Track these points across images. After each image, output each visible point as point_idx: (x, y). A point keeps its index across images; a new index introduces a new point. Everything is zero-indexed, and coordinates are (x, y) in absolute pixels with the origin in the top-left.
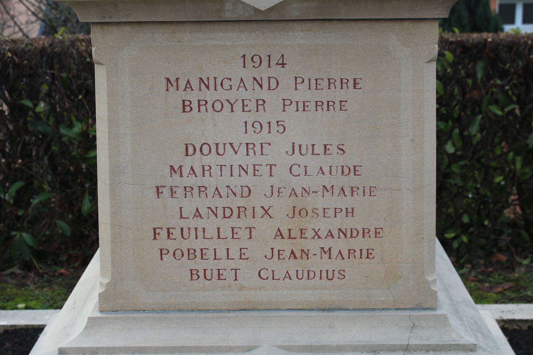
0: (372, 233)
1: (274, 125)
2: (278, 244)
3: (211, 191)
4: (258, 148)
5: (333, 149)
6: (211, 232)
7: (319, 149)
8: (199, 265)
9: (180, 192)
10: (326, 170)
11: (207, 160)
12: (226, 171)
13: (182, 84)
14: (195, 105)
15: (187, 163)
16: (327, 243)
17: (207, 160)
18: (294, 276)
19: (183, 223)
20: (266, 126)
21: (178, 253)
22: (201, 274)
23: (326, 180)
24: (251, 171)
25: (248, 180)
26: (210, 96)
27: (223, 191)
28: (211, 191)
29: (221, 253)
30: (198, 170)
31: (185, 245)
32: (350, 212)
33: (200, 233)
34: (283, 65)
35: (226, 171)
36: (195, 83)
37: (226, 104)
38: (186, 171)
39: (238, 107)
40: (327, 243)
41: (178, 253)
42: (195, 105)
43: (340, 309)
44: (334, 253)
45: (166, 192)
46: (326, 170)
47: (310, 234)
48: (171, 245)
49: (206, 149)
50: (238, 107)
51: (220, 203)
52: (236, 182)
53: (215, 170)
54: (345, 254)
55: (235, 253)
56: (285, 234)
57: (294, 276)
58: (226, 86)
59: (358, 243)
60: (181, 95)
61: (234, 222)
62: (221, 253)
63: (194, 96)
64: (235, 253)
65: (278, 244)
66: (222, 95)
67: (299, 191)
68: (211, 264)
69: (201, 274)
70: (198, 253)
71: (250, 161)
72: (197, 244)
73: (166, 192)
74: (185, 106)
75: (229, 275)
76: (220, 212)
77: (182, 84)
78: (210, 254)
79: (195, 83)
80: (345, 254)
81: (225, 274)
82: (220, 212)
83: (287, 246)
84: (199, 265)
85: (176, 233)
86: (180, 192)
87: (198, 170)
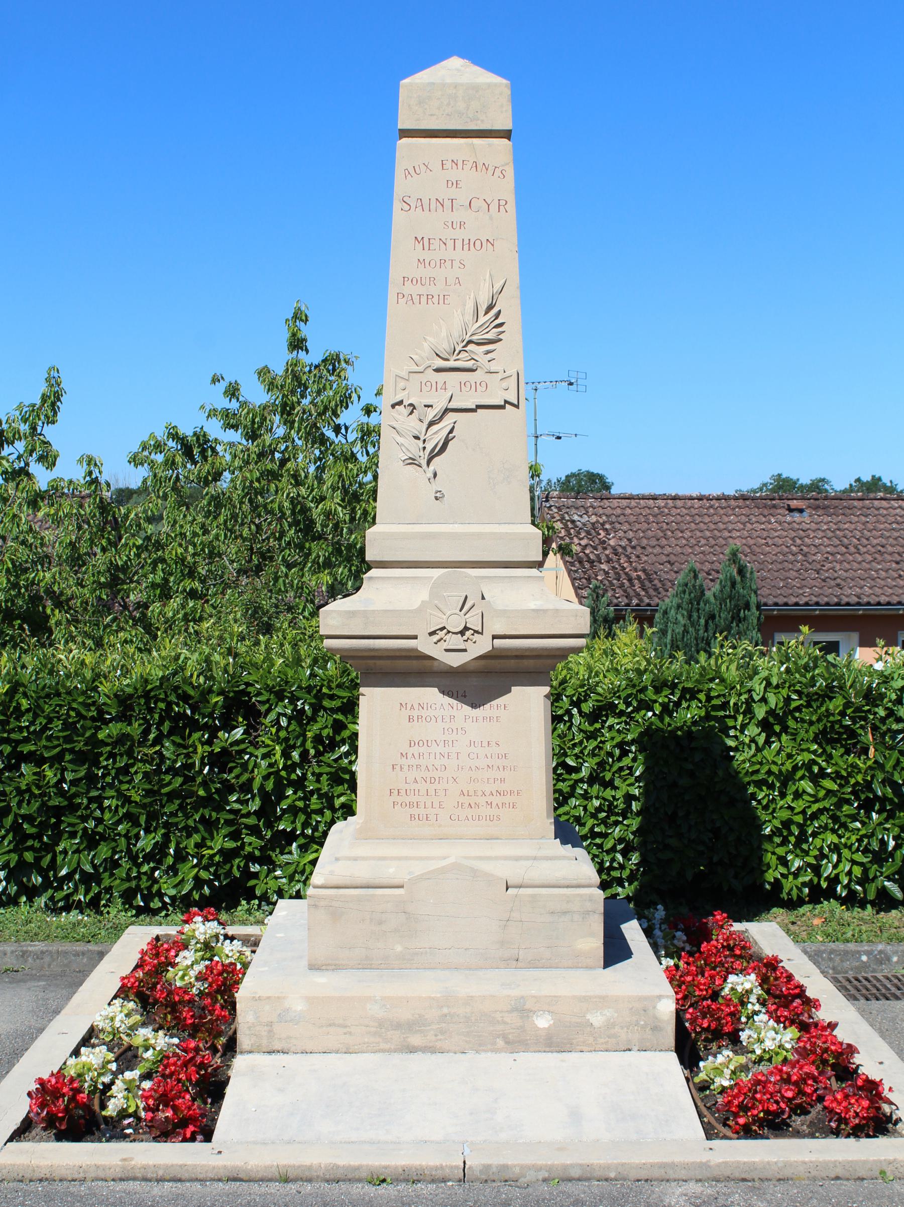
0: (516, 793)
1: (459, 730)
2: (462, 799)
3: (423, 768)
4: (450, 743)
5: (493, 744)
6: (423, 792)
7: (485, 744)
8: (415, 811)
9: (406, 768)
10: (489, 756)
11: (422, 750)
12: (432, 756)
13: (409, 706)
14: (415, 719)
15: (411, 751)
16: (490, 799)
17: (422, 750)
18: (470, 819)
19: (407, 786)
20: (455, 731)
21: (404, 804)
22: (417, 817)
23: (489, 762)
24: (446, 756)
25: (444, 761)
26: (424, 713)
27: (430, 768)
28: (423, 768)
29: (429, 804)
30: (417, 756)
31: (407, 800)
32: (503, 781)
33: (416, 792)
34: (465, 696)
35: (432, 756)
36: (416, 706)
37: (433, 718)
38: (409, 755)
39: (439, 719)
40: (490, 799)
41: (404, 804)
42: (415, 719)
43: (497, 839)
44: (494, 805)
45: (398, 767)
46: (489, 756)
47: (480, 793)
48: (399, 799)
49: (421, 743)
50: (439, 719)
51: (428, 775)
52: (438, 763)
53: (426, 756)
54: (500, 806)
55: (436, 805)
56: (466, 793)
57: (470, 819)
58: (433, 708)
59: (508, 799)
60: (408, 712)
61: (436, 786)
62: (429, 804)
63: (415, 713)
64: (436, 805)
65: (462, 799)
66: (431, 713)
67: (473, 768)
68: (422, 811)
69: (417, 817)
70: (415, 804)
71: (445, 751)
72: (414, 799)
73: (398, 767)
74: (410, 719)
75: (432, 817)
76: (428, 780)
77: (409, 706)
78: (422, 805)
79: (416, 706)
80: (500, 806)
81: (430, 817)
82: (428, 780)
83: (466, 800)
84: (415, 811)
85: (403, 792)
86: (406, 768)
87: (417, 756)
